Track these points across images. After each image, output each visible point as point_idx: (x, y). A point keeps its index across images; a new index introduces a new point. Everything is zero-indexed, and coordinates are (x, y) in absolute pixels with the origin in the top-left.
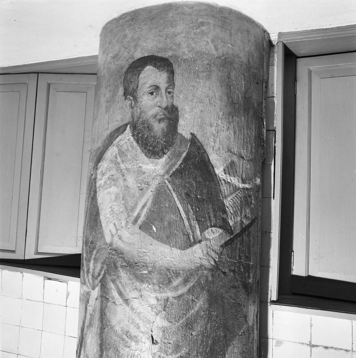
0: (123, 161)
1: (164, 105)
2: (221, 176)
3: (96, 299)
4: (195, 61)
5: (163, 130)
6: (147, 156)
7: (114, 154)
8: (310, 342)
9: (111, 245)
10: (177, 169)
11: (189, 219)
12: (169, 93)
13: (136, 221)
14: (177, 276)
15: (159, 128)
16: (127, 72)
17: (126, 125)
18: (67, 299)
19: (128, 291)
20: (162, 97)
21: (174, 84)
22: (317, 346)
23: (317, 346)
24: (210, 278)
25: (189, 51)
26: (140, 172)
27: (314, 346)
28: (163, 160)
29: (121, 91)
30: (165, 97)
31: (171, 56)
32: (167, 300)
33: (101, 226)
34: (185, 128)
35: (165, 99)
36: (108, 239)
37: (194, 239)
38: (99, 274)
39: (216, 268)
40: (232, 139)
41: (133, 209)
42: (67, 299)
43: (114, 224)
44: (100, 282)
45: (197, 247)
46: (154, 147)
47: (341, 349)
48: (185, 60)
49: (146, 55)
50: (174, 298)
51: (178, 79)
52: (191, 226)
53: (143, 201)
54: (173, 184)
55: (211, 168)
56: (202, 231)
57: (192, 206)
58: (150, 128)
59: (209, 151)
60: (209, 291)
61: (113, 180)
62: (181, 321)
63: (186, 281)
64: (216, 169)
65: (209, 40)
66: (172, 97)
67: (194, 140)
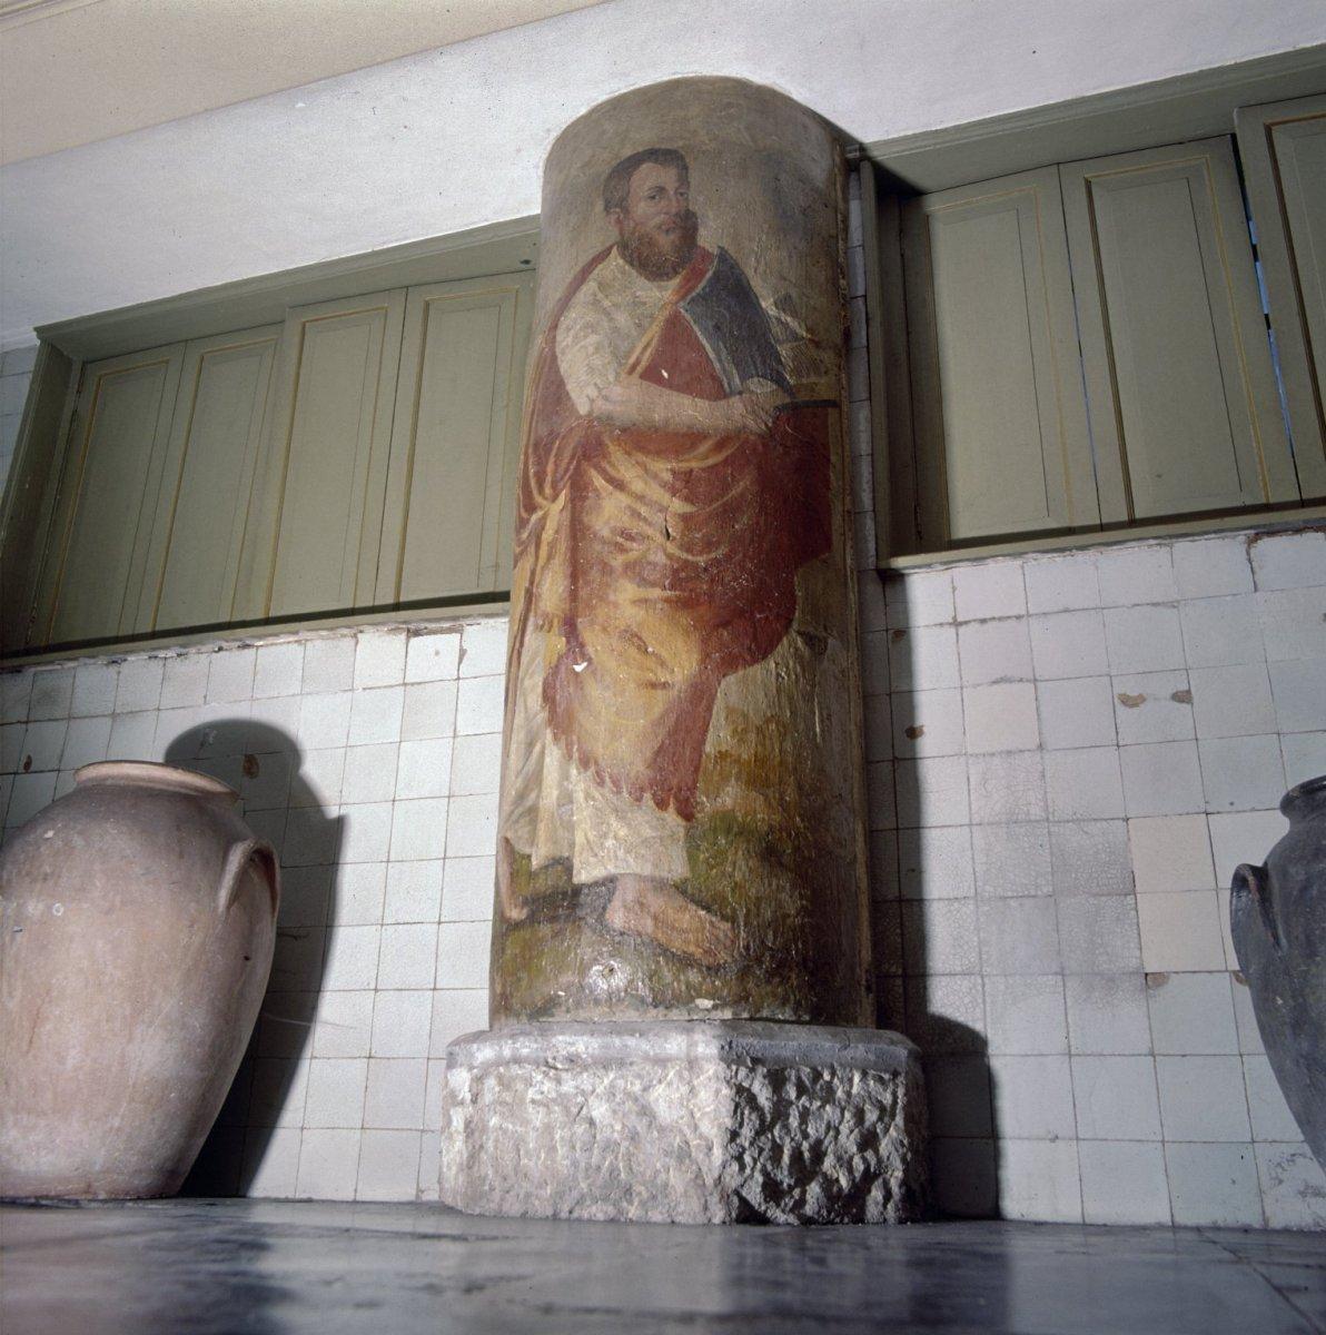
0: (607, 296)
1: (674, 211)
2: (771, 313)
3: (562, 510)
4: (720, 153)
5: (673, 242)
6: (649, 280)
7: (591, 291)
8: (955, 618)
9: (590, 414)
10: (698, 294)
11: (720, 361)
12: (682, 194)
13: (633, 368)
14: (705, 437)
15: (666, 242)
16: (610, 177)
17: (611, 247)
18: (460, 663)
19: (622, 471)
20: (670, 200)
21: (689, 183)
22: (966, 623)
23: (966, 623)
24: (760, 448)
25: (710, 140)
26: (637, 303)
27: (961, 624)
28: (676, 282)
29: (599, 206)
30: (674, 199)
31: (682, 148)
32: (691, 471)
33: (570, 398)
34: (709, 237)
35: (674, 203)
36: (583, 409)
37: (730, 387)
38: (567, 470)
39: (769, 436)
40: (786, 264)
41: (627, 356)
42: (460, 663)
43: (595, 384)
44: (570, 478)
45: (735, 400)
46: (659, 268)
47: (1009, 617)
48: (704, 153)
49: (641, 149)
50: (703, 470)
51: (694, 177)
52: (724, 370)
53: (645, 340)
54: (693, 314)
55: (753, 297)
56: (743, 379)
57: (725, 344)
58: (651, 243)
59: (750, 273)
60: (759, 468)
61: (591, 328)
62: (715, 506)
63: (720, 445)
64: (761, 300)
65: (741, 127)
66: (687, 199)
67: (723, 256)
